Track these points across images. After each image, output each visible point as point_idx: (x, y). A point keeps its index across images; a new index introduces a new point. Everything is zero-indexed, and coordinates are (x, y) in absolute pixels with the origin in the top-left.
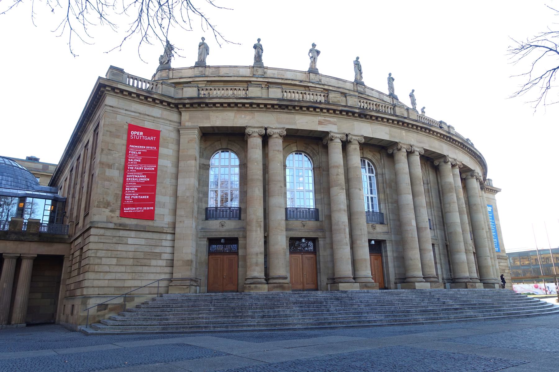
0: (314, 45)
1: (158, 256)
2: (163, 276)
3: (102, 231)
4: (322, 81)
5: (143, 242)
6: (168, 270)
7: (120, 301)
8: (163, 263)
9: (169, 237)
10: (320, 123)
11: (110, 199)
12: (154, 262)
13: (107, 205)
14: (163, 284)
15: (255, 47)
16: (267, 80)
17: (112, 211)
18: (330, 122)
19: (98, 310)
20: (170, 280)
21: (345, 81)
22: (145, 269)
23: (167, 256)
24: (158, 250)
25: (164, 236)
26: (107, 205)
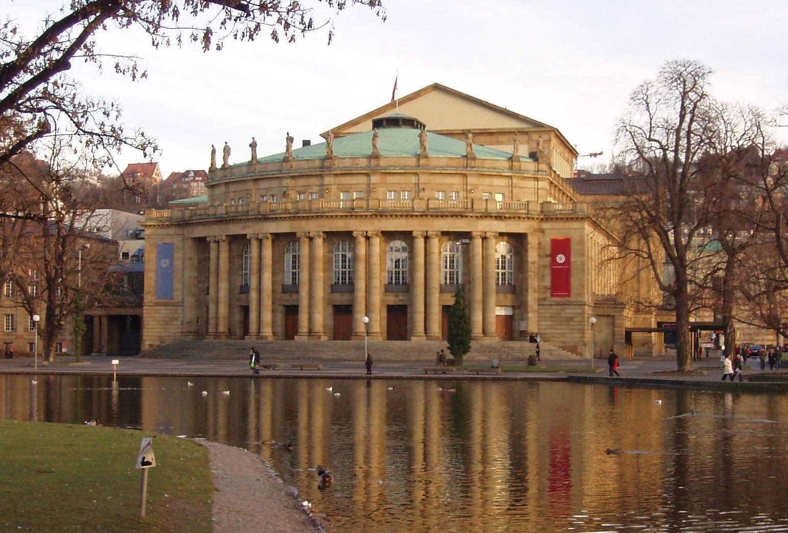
0: (288, 134)
1: (176, 319)
2: (179, 330)
3: (148, 307)
4: (294, 166)
5: (168, 312)
6: (181, 327)
7: (158, 343)
8: (179, 323)
9: (181, 308)
10: (243, 228)
11: (151, 289)
12: (175, 323)
13: (150, 293)
14: (179, 334)
15: (250, 145)
16: (252, 178)
17: (152, 296)
18: (248, 226)
19: (150, 347)
20: (183, 332)
21: (313, 160)
22: (170, 326)
23: (180, 319)
24: (176, 316)
25: (179, 308)
26: (150, 293)
